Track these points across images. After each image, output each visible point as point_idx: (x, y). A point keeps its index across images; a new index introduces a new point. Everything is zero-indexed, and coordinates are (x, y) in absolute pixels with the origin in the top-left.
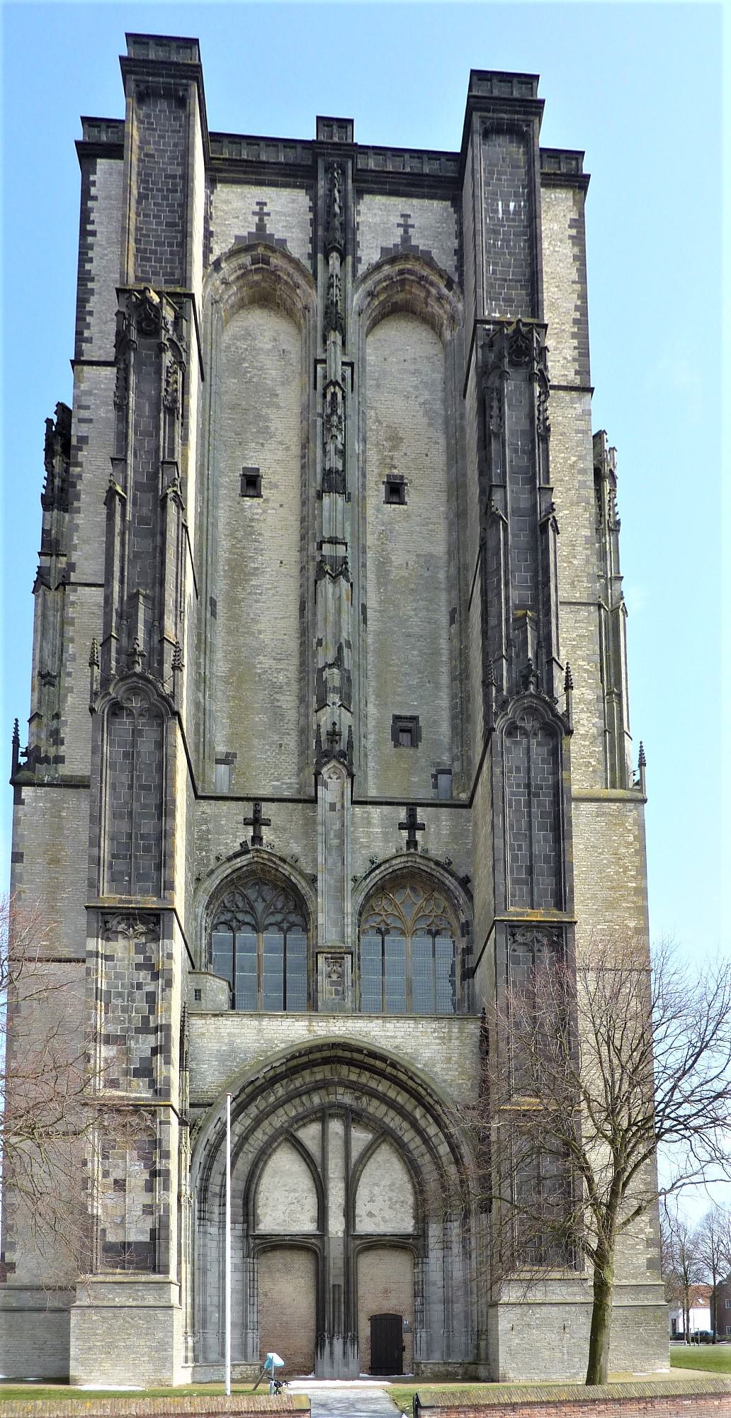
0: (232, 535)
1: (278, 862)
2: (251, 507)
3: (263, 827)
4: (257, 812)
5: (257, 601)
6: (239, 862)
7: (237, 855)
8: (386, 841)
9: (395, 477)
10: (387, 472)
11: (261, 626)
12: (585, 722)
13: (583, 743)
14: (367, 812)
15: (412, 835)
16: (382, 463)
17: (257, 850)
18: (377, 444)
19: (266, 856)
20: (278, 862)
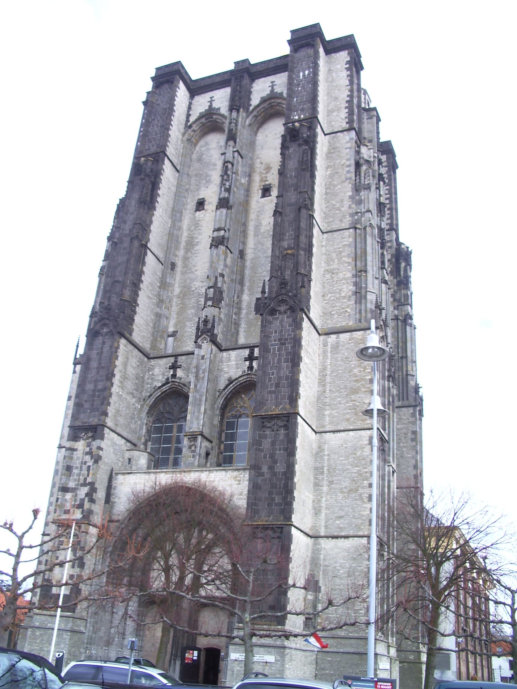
0: (189, 229)
1: (182, 386)
2: (199, 215)
3: (178, 369)
4: (176, 361)
5: (196, 257)
6: (164, 388)
7: (163, 385)
8: (238, 368)
9: (267, 185)
10: (263, 184)
11: (196, 268)
12: (345, 290)
13: (343, 301)
14: (229, 354)
15: (251, 364)
16: (261, 181)
17: (173, 381)
18: (260, 172)
19: (177, 384)
20: (182, 386)
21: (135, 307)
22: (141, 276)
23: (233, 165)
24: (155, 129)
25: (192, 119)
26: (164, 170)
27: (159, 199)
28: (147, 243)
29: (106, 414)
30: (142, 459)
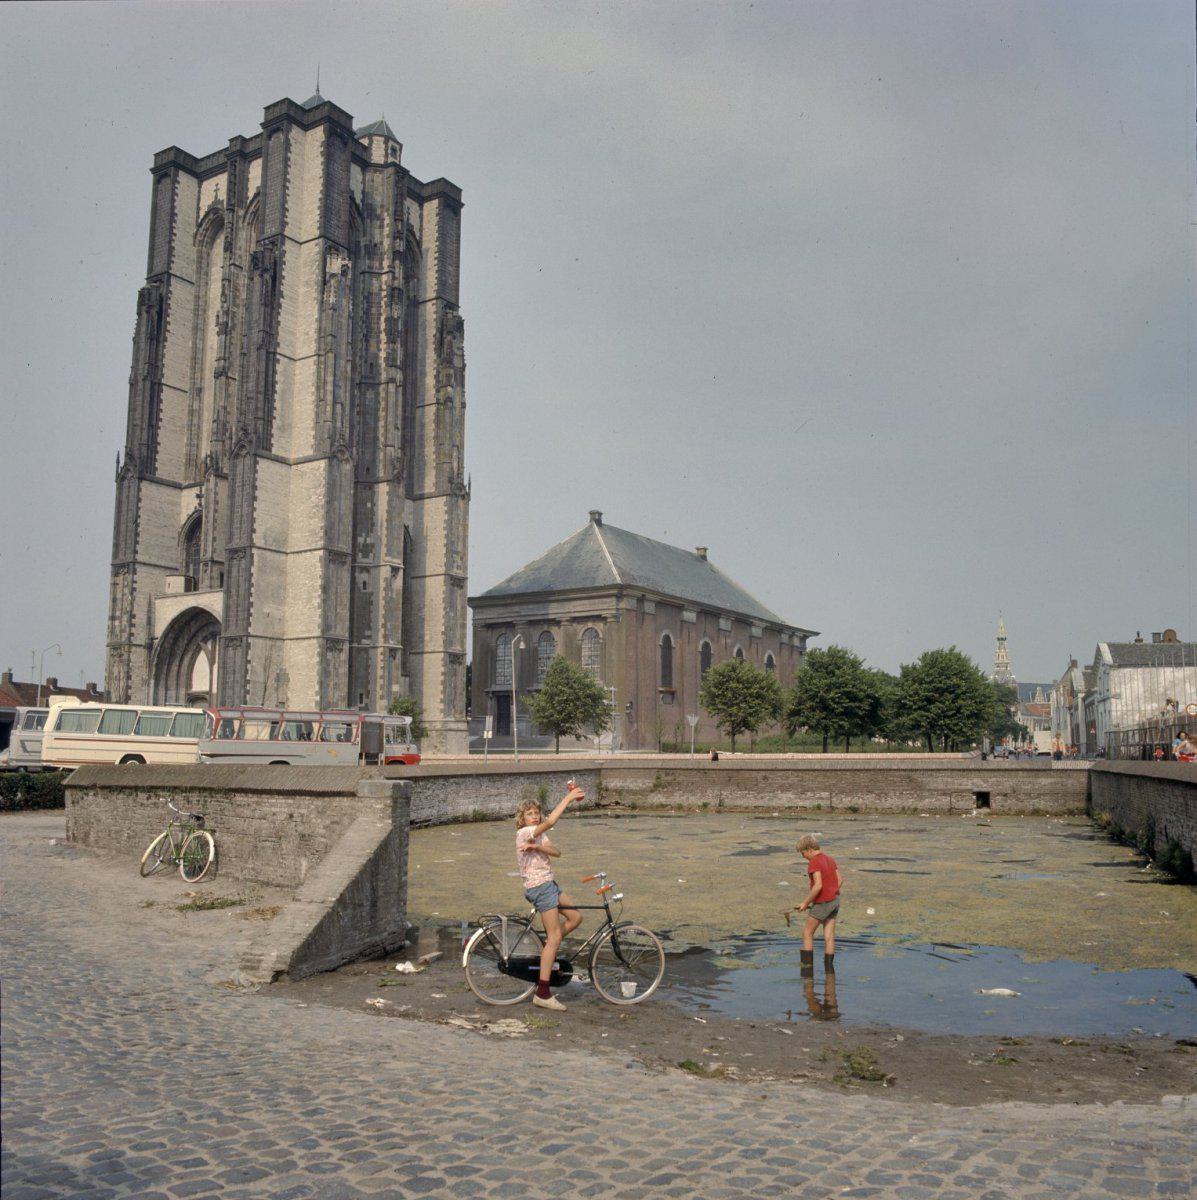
21: (156, 447)
22: (158, 415)
23: (229, 281)
24: (161, 240)
25: (202, 215)
26: (171, 292)
27: (169, 327)
28: (160, 380)
29: (136, 552)
30: (177, 583)
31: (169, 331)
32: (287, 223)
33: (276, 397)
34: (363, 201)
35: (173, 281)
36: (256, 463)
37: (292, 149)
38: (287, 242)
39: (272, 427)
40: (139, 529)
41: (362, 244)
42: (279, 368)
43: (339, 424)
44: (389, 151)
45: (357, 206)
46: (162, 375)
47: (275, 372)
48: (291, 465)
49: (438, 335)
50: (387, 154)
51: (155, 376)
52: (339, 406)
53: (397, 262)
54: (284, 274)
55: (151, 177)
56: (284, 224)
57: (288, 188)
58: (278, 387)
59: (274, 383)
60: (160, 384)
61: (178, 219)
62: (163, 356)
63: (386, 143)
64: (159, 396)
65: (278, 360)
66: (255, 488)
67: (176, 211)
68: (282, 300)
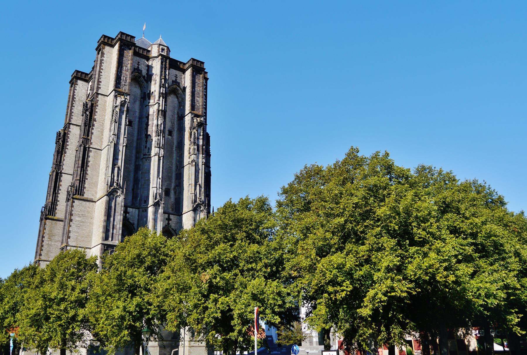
26: (70, 132)
28: (61, 171)
31: (67, 149)
32: (100, 88)
33: (88, 168)
34: (146, 74)
35: (71, 126)
36: (73, 202)
37: (105, 56)
38: (100, 96)
39: (85, 183)
40: (43, 243)
41: (147, 93)
42: (91, 154)
43: (116, 178)
44: (160, 50)
45: (144, 77)
46: (63, 169)
47: (88, 156)
48: (96, 202)
49: (190, 130)
50: (159, 52)
51: (59, 169)
52: (116, 169)
53: (161, 98)
54: (97, 110)
55: (70, 85)
56: (98, 88)
57: (101, 72)
58: (89, 164)
59: (88, 162)
60: (61, 173)
61: (77, 99)
62: (64, 160)
63: (159, 47)
64: (60, 178)
65: (91, 150)
66: (71, 215)
67: (75, 97)
68: (95, 122)
